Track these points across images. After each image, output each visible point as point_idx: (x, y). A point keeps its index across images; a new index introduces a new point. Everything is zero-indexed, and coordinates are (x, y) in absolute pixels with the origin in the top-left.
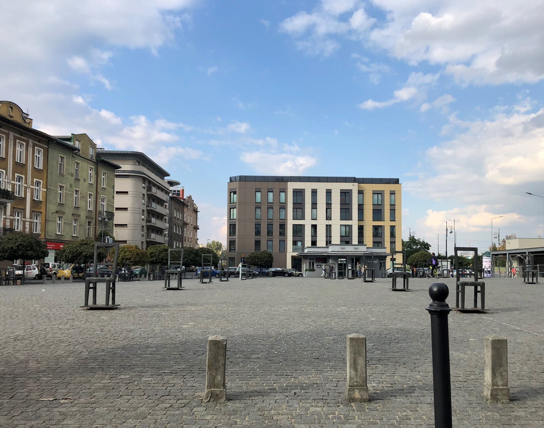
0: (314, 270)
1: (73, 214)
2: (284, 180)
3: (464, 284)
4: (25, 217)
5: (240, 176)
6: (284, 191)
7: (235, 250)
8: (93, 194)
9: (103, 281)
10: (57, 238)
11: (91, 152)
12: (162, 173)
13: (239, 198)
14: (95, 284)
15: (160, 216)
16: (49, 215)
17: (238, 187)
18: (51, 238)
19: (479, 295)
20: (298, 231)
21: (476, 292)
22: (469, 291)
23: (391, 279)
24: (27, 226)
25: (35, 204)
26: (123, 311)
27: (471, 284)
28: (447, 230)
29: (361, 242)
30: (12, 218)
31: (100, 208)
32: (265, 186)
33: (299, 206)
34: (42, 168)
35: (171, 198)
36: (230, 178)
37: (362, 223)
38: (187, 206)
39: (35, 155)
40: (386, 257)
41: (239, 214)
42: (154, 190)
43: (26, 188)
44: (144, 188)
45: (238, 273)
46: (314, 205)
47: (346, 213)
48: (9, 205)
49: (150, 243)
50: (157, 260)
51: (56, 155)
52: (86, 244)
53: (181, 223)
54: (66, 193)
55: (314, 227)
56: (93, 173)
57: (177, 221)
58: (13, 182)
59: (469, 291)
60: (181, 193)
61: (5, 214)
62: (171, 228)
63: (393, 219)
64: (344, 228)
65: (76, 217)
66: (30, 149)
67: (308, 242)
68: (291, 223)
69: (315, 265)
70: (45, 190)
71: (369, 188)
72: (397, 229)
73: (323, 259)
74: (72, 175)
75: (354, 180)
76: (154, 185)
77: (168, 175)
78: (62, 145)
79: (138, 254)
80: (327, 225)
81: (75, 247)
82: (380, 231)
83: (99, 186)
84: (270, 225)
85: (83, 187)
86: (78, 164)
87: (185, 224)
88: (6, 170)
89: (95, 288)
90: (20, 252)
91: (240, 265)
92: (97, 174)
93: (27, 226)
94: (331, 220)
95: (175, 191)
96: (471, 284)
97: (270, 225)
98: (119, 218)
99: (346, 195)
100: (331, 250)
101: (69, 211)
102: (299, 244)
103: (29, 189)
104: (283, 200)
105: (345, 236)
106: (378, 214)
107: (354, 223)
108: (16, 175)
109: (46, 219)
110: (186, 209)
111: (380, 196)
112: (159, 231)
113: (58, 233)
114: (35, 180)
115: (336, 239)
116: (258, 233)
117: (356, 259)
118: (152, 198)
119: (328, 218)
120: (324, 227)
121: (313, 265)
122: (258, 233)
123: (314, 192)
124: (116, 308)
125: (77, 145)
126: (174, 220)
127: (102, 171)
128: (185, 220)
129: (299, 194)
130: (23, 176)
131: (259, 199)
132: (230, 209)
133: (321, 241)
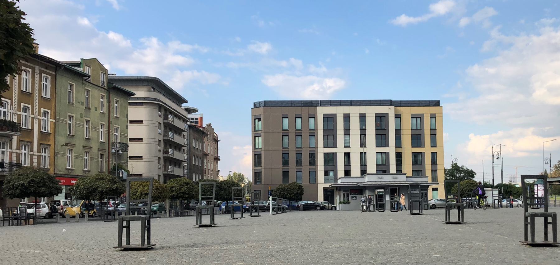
0: (349, 203)
1: (84, 147)
2: (313, 104)
3: (533, 216)
4: (32, 150)
5: (265, 101)
6: (314, 116)
7: (260, 182)
8: (106, 123)
9: (138, 219)
10: (67, 173)
11: (102, 78)
12: (179, 100)
13: (264, 125)
14: (128, 223)
15: (178, 147)
17: (263, 113)
18: (61, 173)
19: (550, 227)
20: (330, 159)
21: (546, 224)
22: (539, 222)
23: (444, 211)
24: (35, 160)
25: (43, 135)
26: (161, 252)
27: (541, 215)
28: (493, 156)
29: (399, 170)
30: (18, 151)
31: (113, 140)
32: (292, 111)
33: (330, 133)
34: (49, 97)
35: (190, 127)
36: (254, 103)
37: (399, 150)
38: (207, 135)
39: (42, 82)
40: (428, 186)
41: (264, 142)
42: (171, 118)
43: (33, 119)
44: (160, 116)
45: (268, 208)
46: (347, 132)
47: (382, 139)
48: (15, 138)
49: (168, 177)
50: (178, 194)
51: (64, 82)
52: (101, 179)
53: (200, 154)
54: (76, 124)
55: (348, 155)
56: (104, 101)
57: (196, 152)
58: (19, 113)
59: (539, 222)
60: (199, 121)
61: (11, 148)
62: (189, 160)
63: (434, 145)
64: (380, 156)
65: (87, 149)
66: (37, 77)
67: (341, 172)
68: (321, 151)
69: (350, 196)
70: (54, 121)
71: (406, 112)
72: (438, 156)
73: (358, 190)
74: (82, 104)
75: (390, 103)
76: (171, 113)
77: (185, 101)
78: (70, 70)
79: (158, 189)
80: (361, 153)
81: (90, 182)
82: (420, 158)
83: (111, 114)
84: (299, 155)
85: (94, 116)
86: (88, 91)
87: (205, 155)
88: (11, 99)
89: (128, 227)
90: (32, 189)
91: (271, 198)
92: (109, 102)
93: (35, 160)
94: (365, 147)
95: (192, 119)
96: (541, 215)
97: (299, 155)
98: (134, 149)
99: (381, 119)
100: (367, 180)
101: (79, 143)
102: (331, 174)
103: (36, 120)
104: (312, 127)
105: (382, 165)
106: (417, 140)
107: (392, 150)
108: (22, 104)
110: (205, 139)
111: (419, 120)
112: (177, 163)
113: (68, 167)
114: (43, 109)
115: (372, 168)
116: (286, 163)
117: (394, 190)
118: (169, 127)
119: (363, 144)
120: (359, 155)
121: (348, 196)
122: (286, 163)
123: (347, 117)
124: (152, 249)
125: (87, 70)
126: (192, 150)
127: (114, 98)
128: (205, 150)
129: (330, 119)
130: (30, 106)
131: (299, 126)
132: (255, 137)
133: (356, 171)
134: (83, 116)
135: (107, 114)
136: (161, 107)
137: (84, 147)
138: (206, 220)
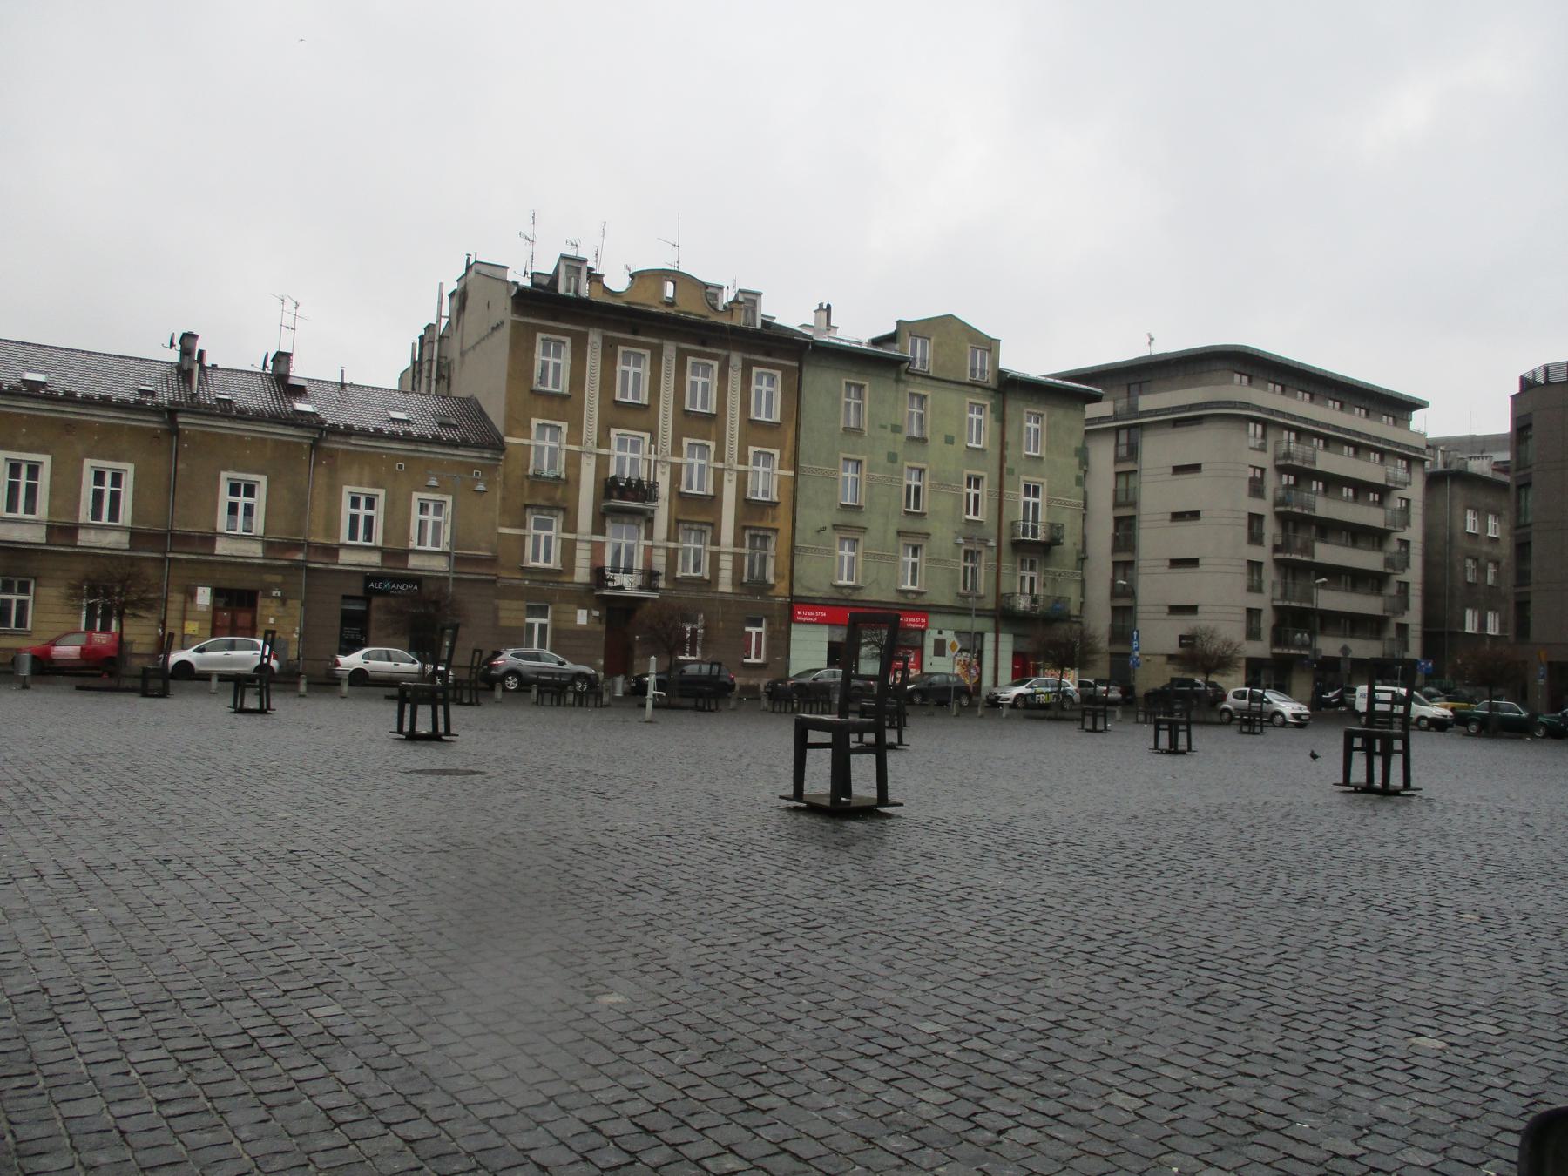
1: (899, 533)
5: (1547, 369)
10: (902, 600)
16: (805, 537)
56: (986, 418)
70: (791, 473)
109: (793, 547)
118: (1304, 475)
134: (900, 459)
135: (997, 451)
136: (1269, 423)
137: (899, 533)
138: (252, 702)
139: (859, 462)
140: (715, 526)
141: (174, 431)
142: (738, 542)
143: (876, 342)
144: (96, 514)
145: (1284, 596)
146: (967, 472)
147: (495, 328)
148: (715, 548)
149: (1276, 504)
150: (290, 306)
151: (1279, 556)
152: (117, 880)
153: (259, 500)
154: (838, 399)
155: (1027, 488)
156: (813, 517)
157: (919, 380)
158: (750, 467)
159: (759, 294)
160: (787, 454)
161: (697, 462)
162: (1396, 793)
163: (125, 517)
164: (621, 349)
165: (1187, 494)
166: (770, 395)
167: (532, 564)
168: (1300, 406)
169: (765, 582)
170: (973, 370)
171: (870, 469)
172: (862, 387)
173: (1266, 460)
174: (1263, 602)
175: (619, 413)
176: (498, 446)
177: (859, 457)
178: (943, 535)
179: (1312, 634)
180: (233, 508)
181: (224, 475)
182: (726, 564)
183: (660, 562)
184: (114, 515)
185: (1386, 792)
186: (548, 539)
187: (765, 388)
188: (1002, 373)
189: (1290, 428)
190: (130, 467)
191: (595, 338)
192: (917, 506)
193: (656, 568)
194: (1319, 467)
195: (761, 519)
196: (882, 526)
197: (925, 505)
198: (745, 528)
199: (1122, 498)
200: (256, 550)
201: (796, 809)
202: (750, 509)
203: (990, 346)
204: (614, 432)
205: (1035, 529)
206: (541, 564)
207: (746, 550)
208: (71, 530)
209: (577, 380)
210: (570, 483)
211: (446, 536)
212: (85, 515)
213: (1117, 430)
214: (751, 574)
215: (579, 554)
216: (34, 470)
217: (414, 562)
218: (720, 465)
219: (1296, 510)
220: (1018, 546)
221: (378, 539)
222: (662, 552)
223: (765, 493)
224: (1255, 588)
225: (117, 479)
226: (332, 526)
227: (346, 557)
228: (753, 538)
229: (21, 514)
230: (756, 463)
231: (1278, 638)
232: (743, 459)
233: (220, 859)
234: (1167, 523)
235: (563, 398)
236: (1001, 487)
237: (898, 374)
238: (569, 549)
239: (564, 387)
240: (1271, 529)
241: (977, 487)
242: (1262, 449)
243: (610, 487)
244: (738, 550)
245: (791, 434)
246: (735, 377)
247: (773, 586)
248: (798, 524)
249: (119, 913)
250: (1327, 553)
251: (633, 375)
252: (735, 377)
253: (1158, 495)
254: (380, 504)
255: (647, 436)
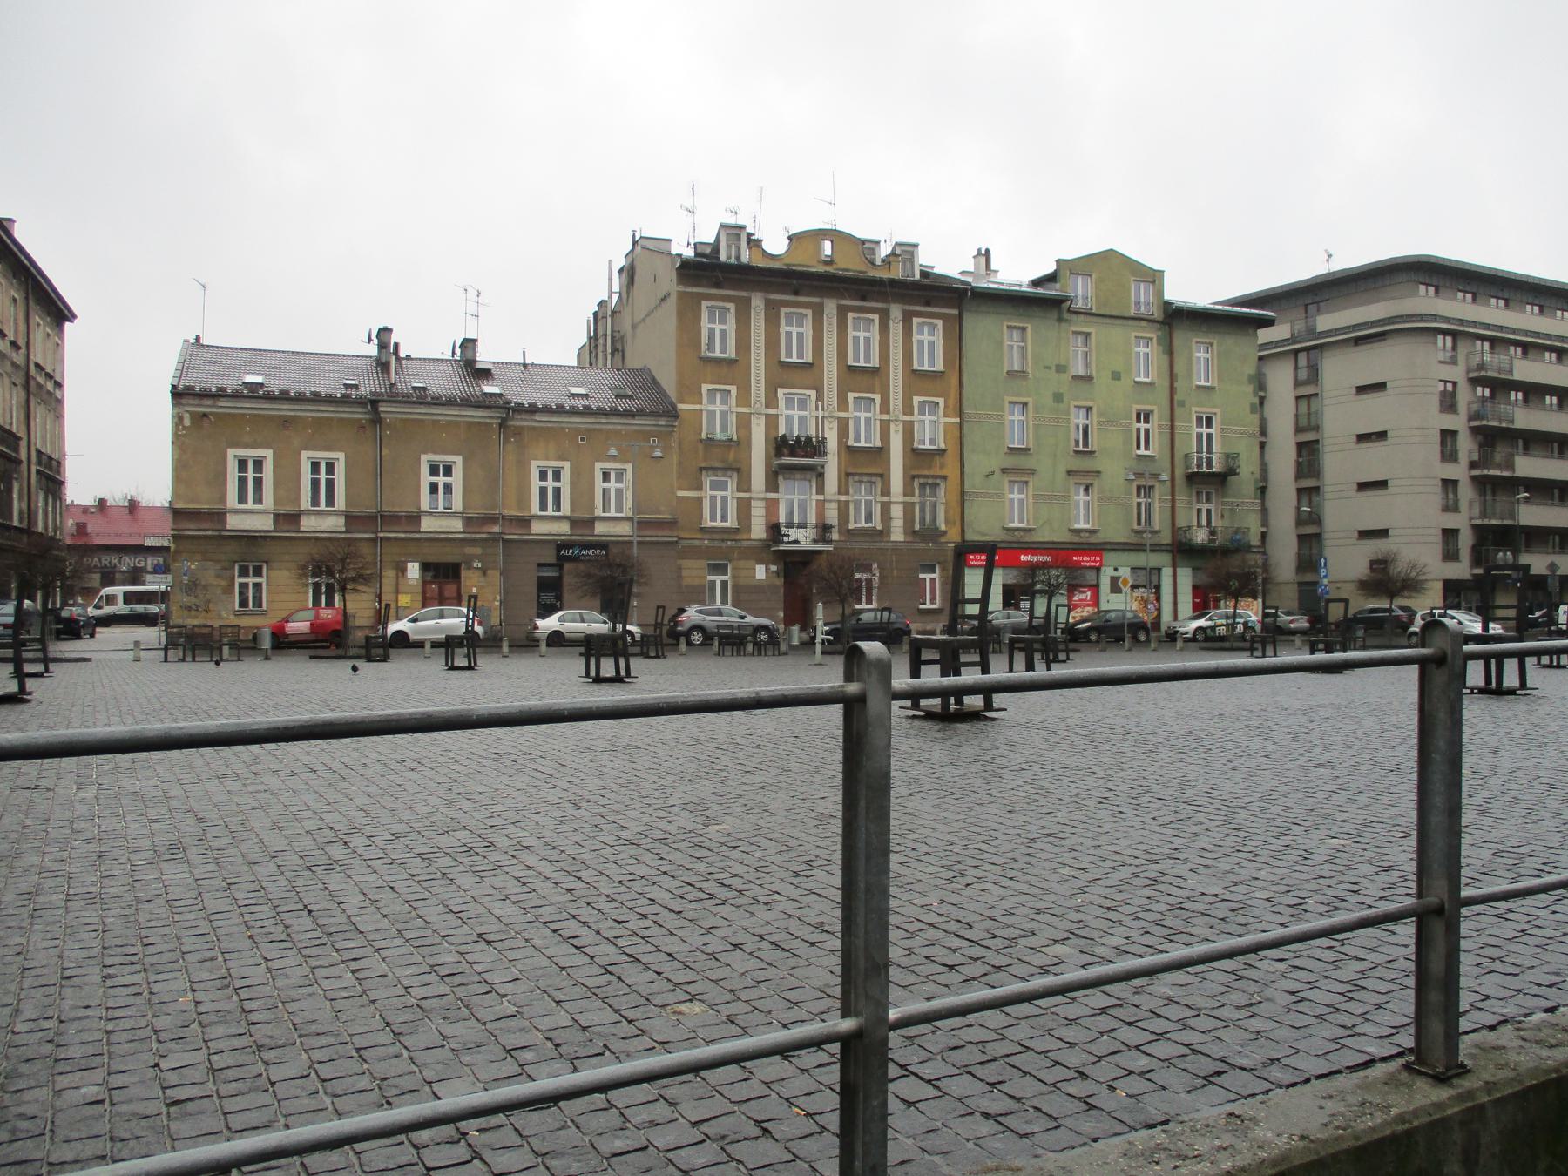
1: (1069, 473)
10: (1076, 539)
54: (1099, 423)
109: (963, 493)
135: (1167, 384)
137: (1069, 473)
139: (1025, 405)
140: (884, 477)
141: (377, 420)
142: (908, 491)
143: (1036, 283)
144: (315, 501)
145: (1483, 515)
146: (1136, 407)
147: (663, 300)
148: (885, 499)
149: (1470, 419)
150: (472, 294)
151: (1476, 472)
152: (369, 772)
153: (457, 479)
154: (1000, 344)
155: (1199, 419)
156: (981, 462)
157: (1082, 317)
158: (916, 417)
159: (916, 246)
160: (951, 402)
161: (863, 415)
162: (1512, 692)
163: (340, 502)
164: (783, 311)
165: (1372, 415)
166: (932, 344)
167: (710, 524)
168: (1493, 313)
169: (937, 529)
170: (1137, 303)
171: (1036, 410)
172: (1024, 329)
173: (1458, 373)
174: (1460, 521)
175: (785, 373)
176: (672, 413)
177: (1024, 400)
178: (1114, 471)
179: (1516, 553)
180: (434, 488)
181: (424, 458)
182: (897, 513)
183: (832, 515)
184: (330, 500)
185: (1501, 692)
186: (724, 499)
187: (926, 338)
188: (1167, 304)
189: (1483, 338)
190: (341, 456)
191: (757, 302)
192: (1086, 445)
193: (828, 521)
194: (1517, 376)
195: (930, 467)
196: (1050, 467)
197: (1094, 443)
198: (914, 477)
199: (1303, 422)
200: (457, 525)
201: (914, 717)
202: (918, 457)
203: (1154, 278)
204: (780, 391)
205: (1209, 461)
206: (719, 524)
207: (916, 499)
208: (294, 518)
209: (743, 344)
210: (741, 444)
211: (628, 503)
212: (305, 503)
213: (1296, 352)
214: (923, 519)
215: (754, 512)
216: (259, 464)
217: (600, 528)
218: (885, 417)
219: (1495, 423)
220: (1192, 478)
221: (566, 509)
222: (834, 505)
223: (932, 441)
224: (1451, 507)
225: (330, 468)
226: (524, 500)
227: (538, 528)
228: (923, 486)
229: (250, 505)
230: (922, 412)
231: (1478, 558)
232: (908, 409)
233: (441, 759)
234: (1353, 446)
235: (731, 362)
236: (1172, 420)
237: (1060, 312)
238: (744, 508)
239: (731, 353)
240: (1466, 446)
241: (1146, 421)
242: (1453, 361)
243: (781, 446)
244: (908, 499)
245: (954, 381)
246: (896, 329)
247: (945, 533)
248: (966, 469)
249: (373, 789)
250: (1528, 466)
251: (797, 333)
252: (896, 329)
253: (1341, 417)
254: (566, 476)
255: (813, 393)
